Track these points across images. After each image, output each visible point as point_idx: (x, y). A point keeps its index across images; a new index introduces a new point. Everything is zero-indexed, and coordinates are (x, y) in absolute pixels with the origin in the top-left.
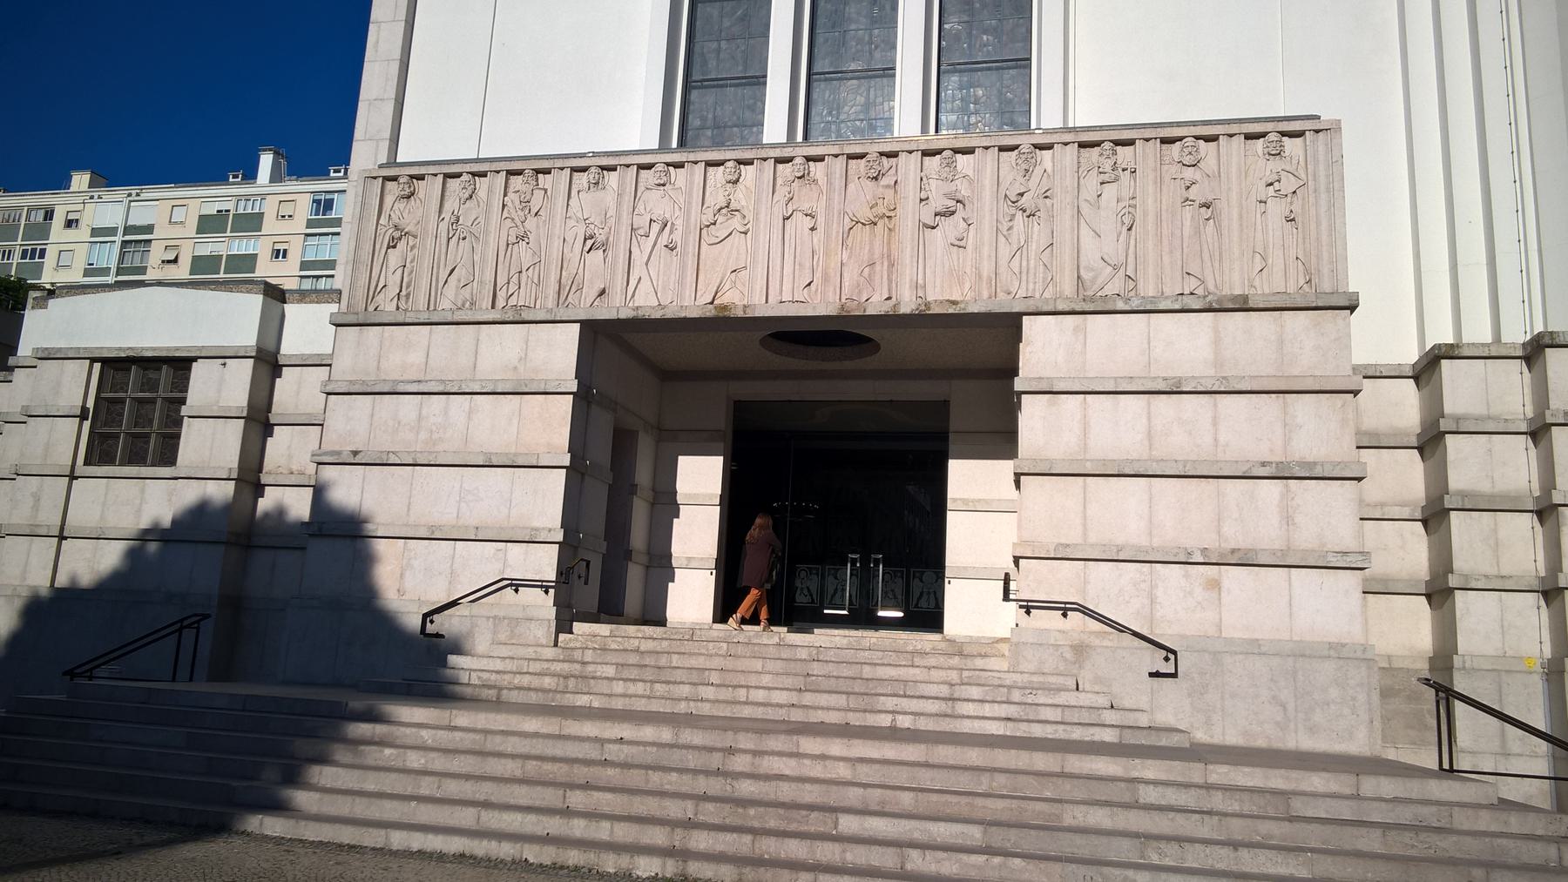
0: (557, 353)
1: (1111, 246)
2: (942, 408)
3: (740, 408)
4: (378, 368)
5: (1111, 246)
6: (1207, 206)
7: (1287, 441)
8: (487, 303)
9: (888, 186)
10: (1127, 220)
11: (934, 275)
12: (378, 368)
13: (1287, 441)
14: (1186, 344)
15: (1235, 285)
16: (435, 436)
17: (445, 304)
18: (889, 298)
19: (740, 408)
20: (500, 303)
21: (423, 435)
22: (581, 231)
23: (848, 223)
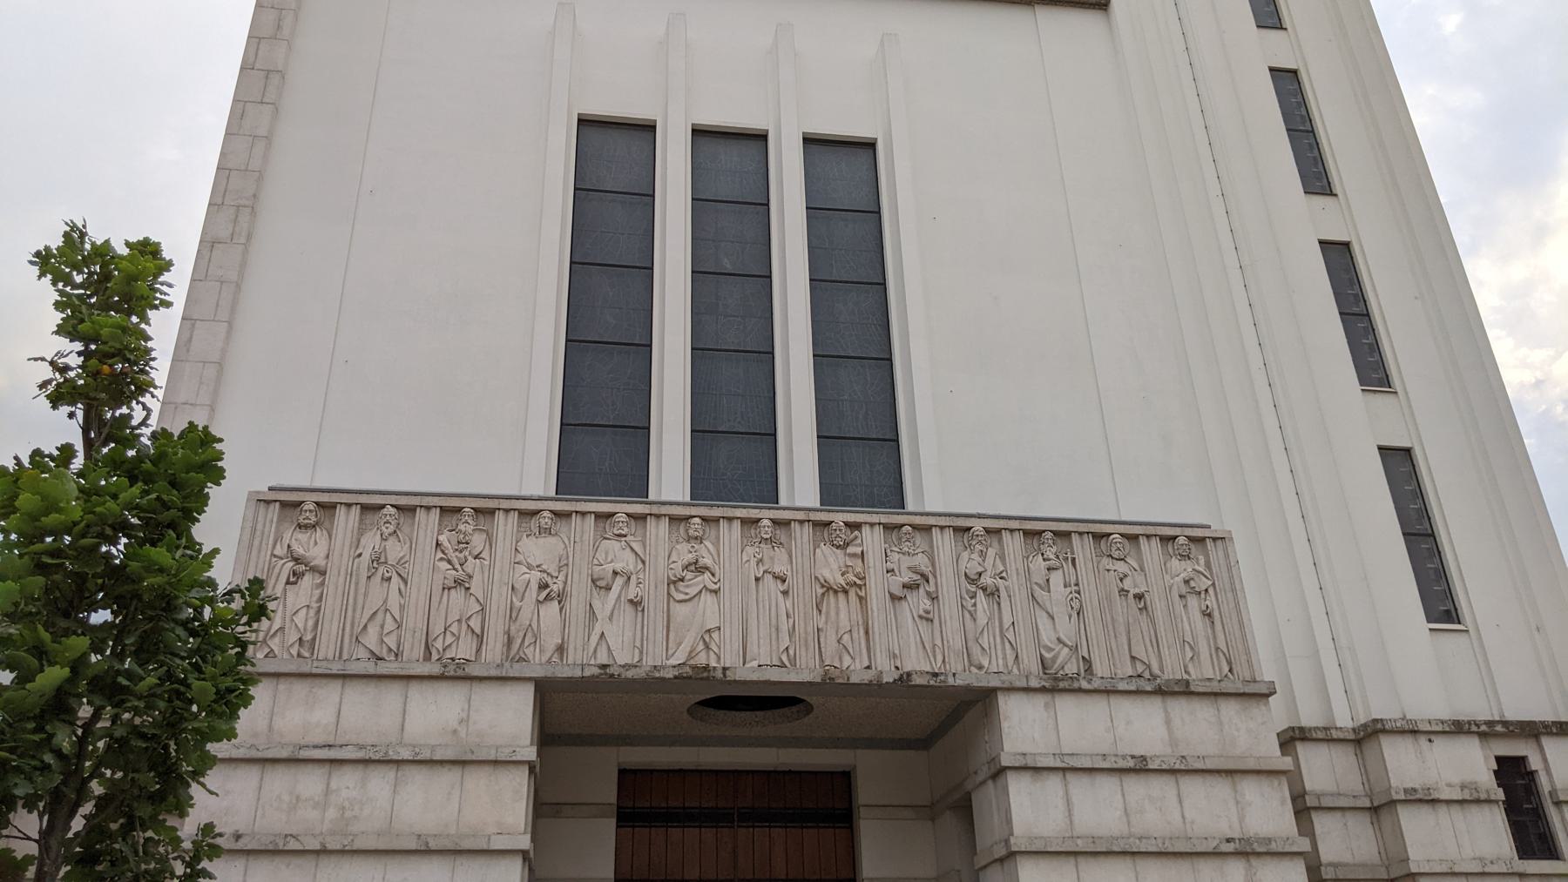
0: (509, 719)
1: (1066, 628)
2: (843, 780)
3: (628, 777)
4: (270, 727)
5: (1066, 628)
6: (1139, 597)
7: (1241, 819)
8: (420, 651)
9: (854, 555)
10: (1076, 604)
11: (900, 644)
12: (270, 727)
13: (1241, 819)
14: (1143, 727)
15: (1172, 671)
16: (348, 814)
17: (326, 648)
18: (868, 667)
19: (628, 777)
20: (435, 656)
21: (332, 813)
22: (536, 576)
23: (820, 591)
